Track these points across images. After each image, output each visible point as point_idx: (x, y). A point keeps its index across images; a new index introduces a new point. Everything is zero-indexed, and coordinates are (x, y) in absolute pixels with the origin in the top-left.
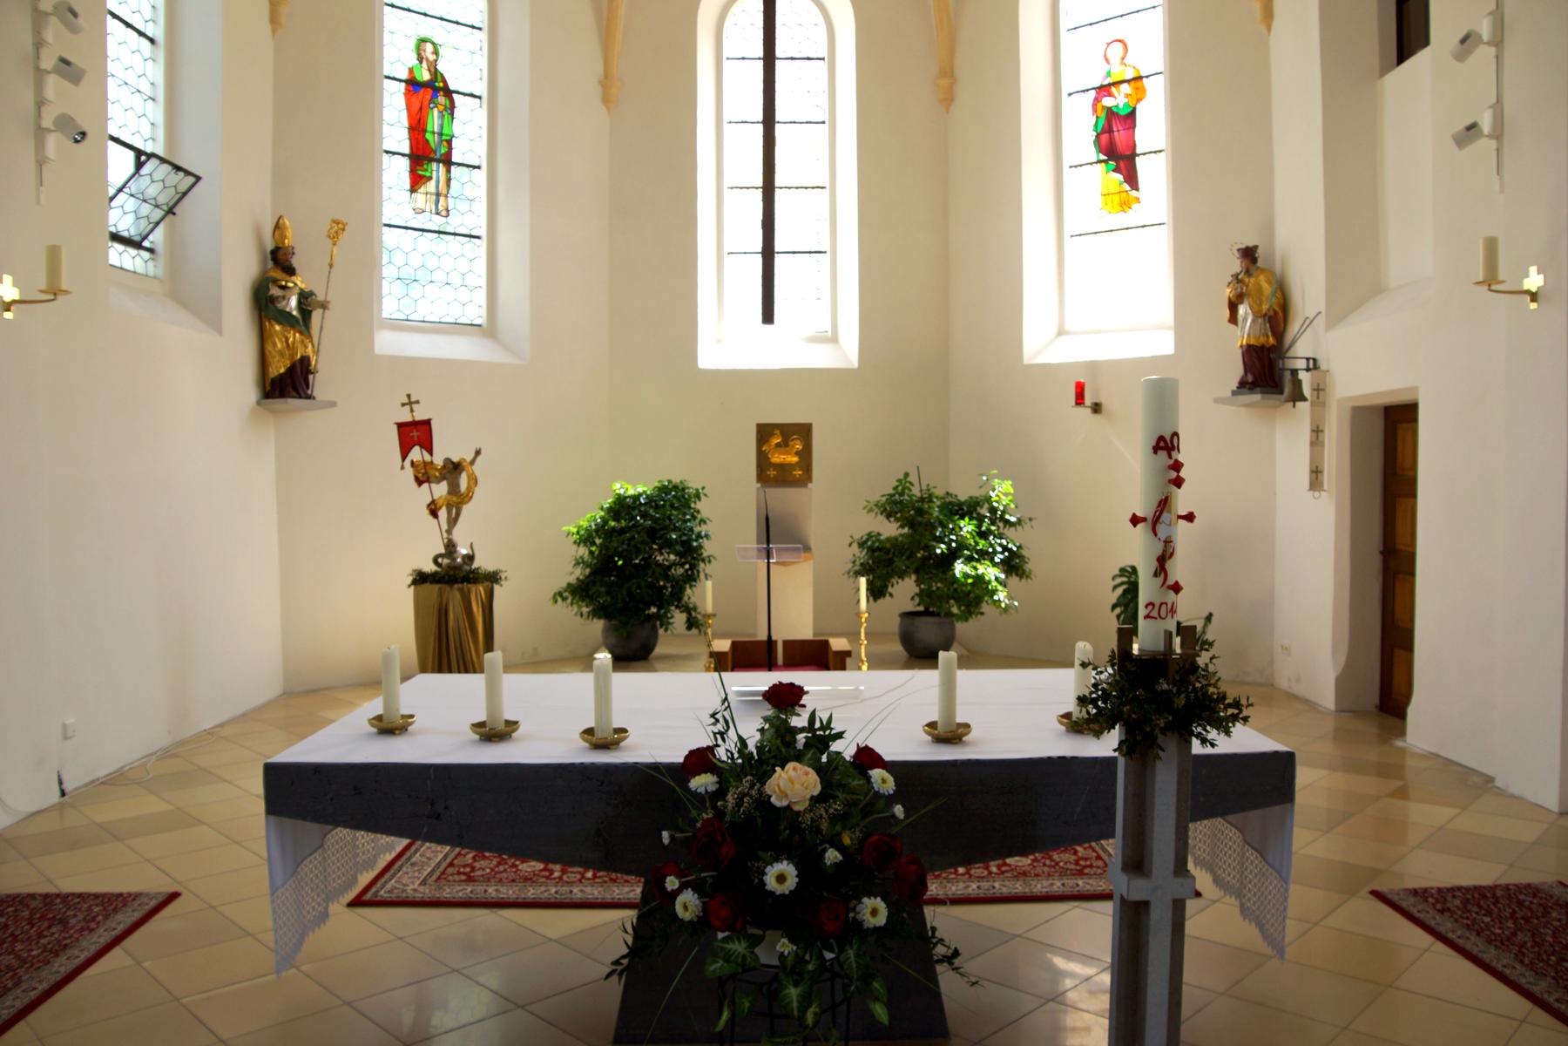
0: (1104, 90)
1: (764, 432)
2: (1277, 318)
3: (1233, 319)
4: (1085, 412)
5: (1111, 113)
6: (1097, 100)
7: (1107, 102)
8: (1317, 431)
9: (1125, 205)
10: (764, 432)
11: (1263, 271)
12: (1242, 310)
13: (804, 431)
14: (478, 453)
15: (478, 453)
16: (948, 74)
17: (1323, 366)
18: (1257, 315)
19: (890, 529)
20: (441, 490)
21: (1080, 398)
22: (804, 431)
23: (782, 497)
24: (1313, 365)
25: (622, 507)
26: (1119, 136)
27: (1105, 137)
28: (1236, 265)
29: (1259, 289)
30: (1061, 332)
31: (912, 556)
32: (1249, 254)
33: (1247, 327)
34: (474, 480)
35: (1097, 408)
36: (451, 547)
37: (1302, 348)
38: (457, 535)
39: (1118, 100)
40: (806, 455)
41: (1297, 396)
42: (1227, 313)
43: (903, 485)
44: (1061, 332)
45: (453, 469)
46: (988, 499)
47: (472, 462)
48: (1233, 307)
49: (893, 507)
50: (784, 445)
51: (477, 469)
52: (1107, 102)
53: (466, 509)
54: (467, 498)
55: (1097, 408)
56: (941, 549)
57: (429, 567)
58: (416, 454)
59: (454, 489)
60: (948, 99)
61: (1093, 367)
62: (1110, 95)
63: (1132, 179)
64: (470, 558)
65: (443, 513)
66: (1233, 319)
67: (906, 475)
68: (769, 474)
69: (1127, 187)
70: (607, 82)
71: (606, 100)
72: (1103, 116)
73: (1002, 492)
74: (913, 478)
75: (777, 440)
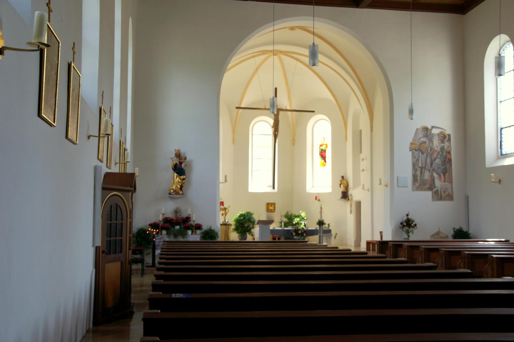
0: (321, 146)
1: (268, 204)
2: (347, 187)
3: (340, 187)
4: (317, 201)
5: (322, 150)
6: (320, 147)
7: (321, 148)
8: (351, 205)
9: (324, 165)
10: (268, 204)
11: (345, 180)
12: (342, 186)
13: (274, 204)
14: (229, 206)
15: (229, 206)
16: (294, 140)
17: (352, 195)
18: (344, 187)
19: (285, 220)
20: (224, 212)
21: (316, 198)
22: (274, 204)
23: (271, 214)
24: (351, 195)
25: (241, 215)
26: (323, 154)
27: (321, 154)
28: (341, 179)
29: (344, 183)
30: (313, 187)
31: (289, 224)
32: (343, 177)
33: (342, 189)
34: (228, 211)
35: (319, 200)
36: (225, 220)
37: (350, 192)
38: (226, 218)
39: (323, 148)
40: (274, 208)
41: (348, 200)
42: (339, 186)
43: (287, 213)
44: (313, 187)
45: (225, 209)
46: (301, 215)
47: (228, 208)
48: (340, 185)
49: (286, 216)
50: (271, 206)
51: (229, 209)
52: (321, 148)
53: (227, 215)
54: (227, 213)
55: (319, 200)
56: (294, 223)
57: (222, 223)
58: (222, 207)
59: (225, 212)
60: (294, 144)
61: (319, 194)
62: (322, 146)
63: (325, 161)
64: (228, 222)
65: (224, 215)
66: (340, 187)
67: (288, 211)
68: (268, 210)
69: (324, 163)
70: (233, 139)
71: (233, 143)
72: (321, 150)
73: (303, 214)
74: (289, 211)
75: (270, 205)
